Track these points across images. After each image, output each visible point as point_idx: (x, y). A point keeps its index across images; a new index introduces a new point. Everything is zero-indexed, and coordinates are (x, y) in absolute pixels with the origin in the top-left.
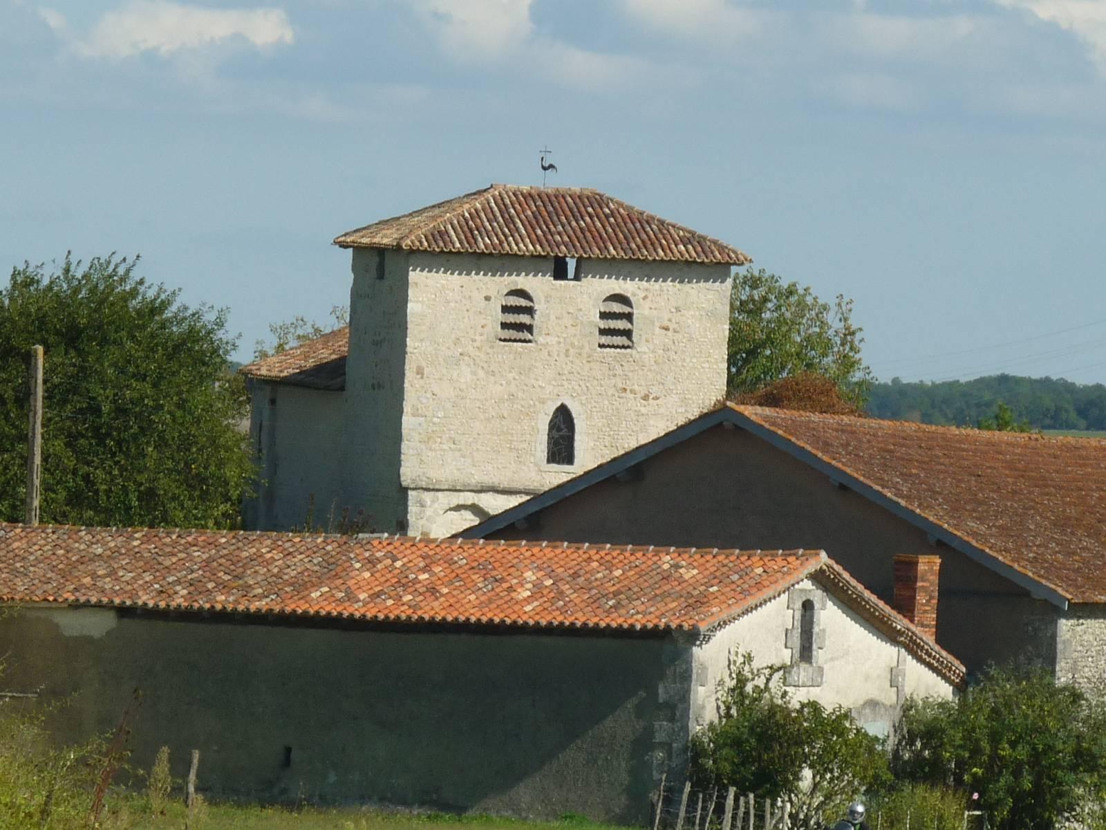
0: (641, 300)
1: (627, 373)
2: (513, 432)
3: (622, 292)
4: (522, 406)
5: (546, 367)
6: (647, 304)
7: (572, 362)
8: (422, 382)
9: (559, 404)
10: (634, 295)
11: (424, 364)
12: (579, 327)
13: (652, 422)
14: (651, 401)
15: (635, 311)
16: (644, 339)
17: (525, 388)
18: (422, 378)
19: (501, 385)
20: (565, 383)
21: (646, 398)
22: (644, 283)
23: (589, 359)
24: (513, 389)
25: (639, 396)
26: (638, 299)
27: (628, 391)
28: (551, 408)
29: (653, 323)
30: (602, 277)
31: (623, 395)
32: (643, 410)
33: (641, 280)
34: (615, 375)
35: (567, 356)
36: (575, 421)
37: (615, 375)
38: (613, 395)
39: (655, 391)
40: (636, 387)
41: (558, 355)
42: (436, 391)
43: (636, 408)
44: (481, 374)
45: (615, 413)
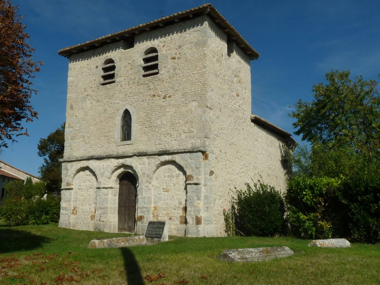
0: (162, 48)
1: (155, 87)
2: (106, 128)
3: (153, 46)
4: (110, 114)
5: (120, 92)
6: (165, 48)
7: (131, 88)
8: (72, 112)
9: (124, 109)
10: (158, 46)
11: (73, 104)
12: (133, 70)
13: (168, 110)
14: (167, 99)
15: (159, 54)
16: (163, 66)
17: (111, 105)
18: (72, 110)
19: (101, 106)
20: (128, 99)
21: (165, 98)
22: (163, 38)
23: (138, 84)
24: (106, 107)
25: (162, 97)
26: (160, 48)
27: (156, 96)
28: (121, 112)
29: (167, 57)
30: (143, 42)
31: (154, 98)
32: (163, 104)
33: (161, 37)
34: (150, 89)
35: (129, 85)
36: (132, 116)
37: (150, 89)
38: (149, 100)
39: (171, 92)
40: (160, 93)
41: (125, 86)
42: (77, 114)
43: (160, 104)
44: (94, 102)
45: (150, 108)
